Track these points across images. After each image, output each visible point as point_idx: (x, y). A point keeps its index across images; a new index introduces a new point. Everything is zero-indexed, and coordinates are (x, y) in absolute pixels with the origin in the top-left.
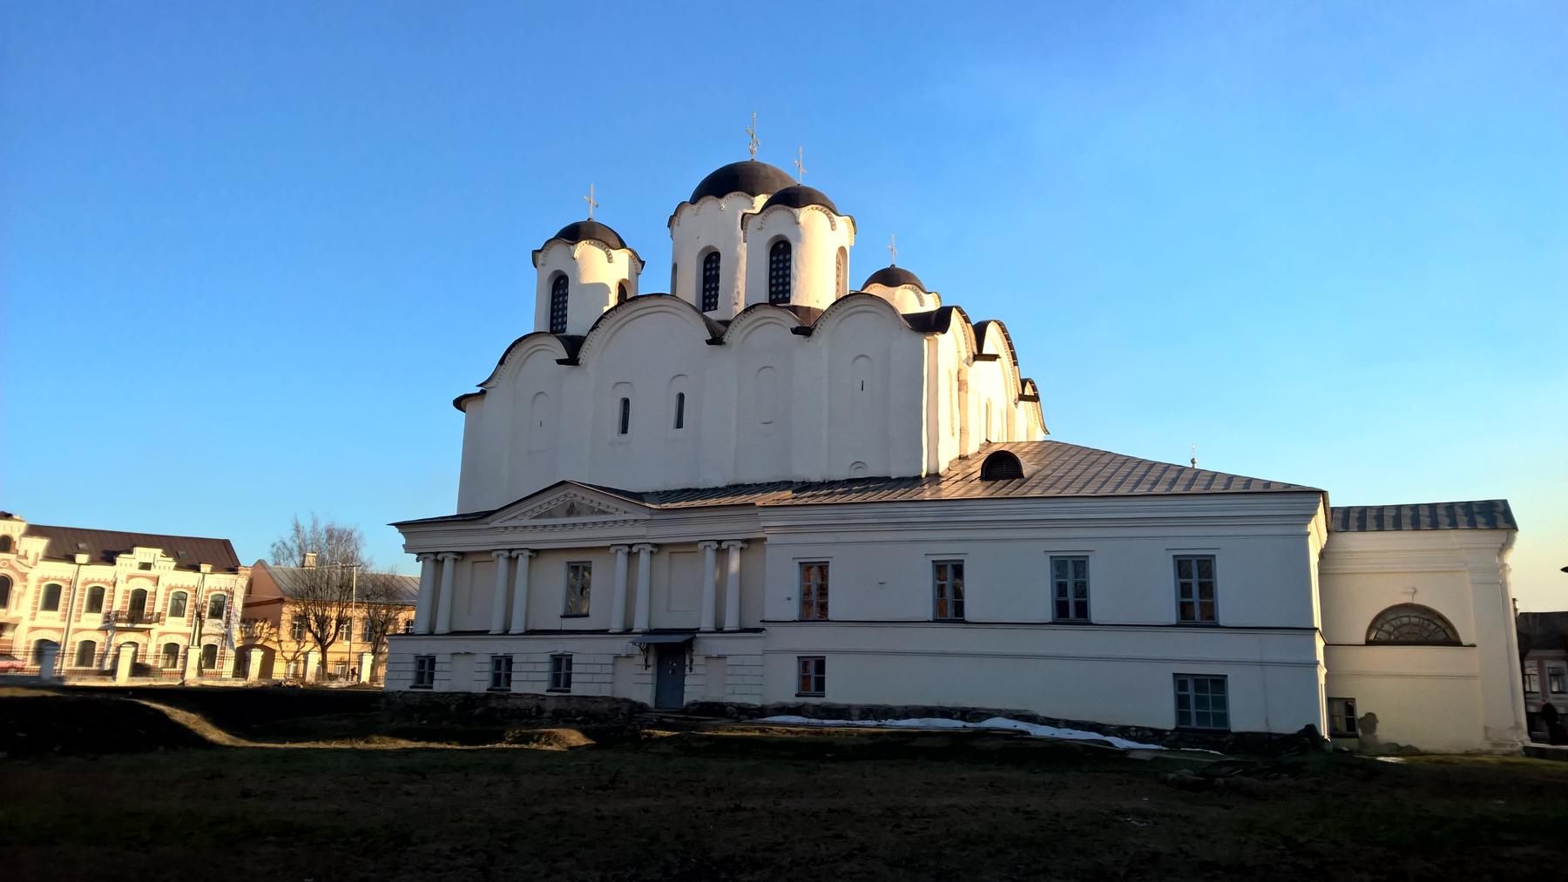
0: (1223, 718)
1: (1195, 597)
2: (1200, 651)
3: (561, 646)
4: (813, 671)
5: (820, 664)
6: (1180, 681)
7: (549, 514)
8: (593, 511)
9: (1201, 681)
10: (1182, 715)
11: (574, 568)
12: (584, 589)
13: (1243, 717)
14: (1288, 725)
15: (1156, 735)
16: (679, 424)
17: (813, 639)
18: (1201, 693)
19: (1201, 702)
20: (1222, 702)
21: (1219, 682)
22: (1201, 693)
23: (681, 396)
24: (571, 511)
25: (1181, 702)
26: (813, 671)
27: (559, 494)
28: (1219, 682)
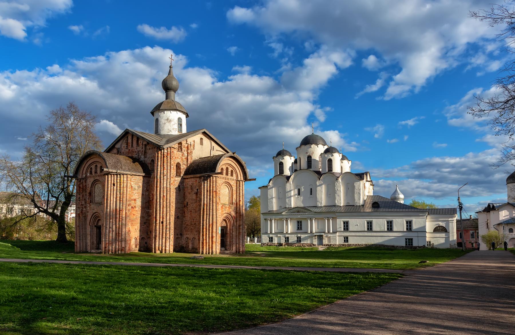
0: (412, 244)
1: (409, 227)
2: (410, 235)
3: (299, 235)
4: (346, 239)
5: (347, 238)
6: (406, 239)
7: (294, 212)
8: (303, 212)
9: (409, 239)
10: (406, 244)
11: (298, 222)
12: (301, 225)
13: (415, 244)
14: (421, 245)
15: (403, 247)
16: (311, 194)
17: (346, 234)
18: (409, 241)
19: (409, 242)
20: (412, 242)
21: (412, 239)
22: (409, 241)
23: (311, 189)
24: (298, 212)
25: (406, 242)
26: (346, 239)
27: (296, 209)
28: (412, 239)
